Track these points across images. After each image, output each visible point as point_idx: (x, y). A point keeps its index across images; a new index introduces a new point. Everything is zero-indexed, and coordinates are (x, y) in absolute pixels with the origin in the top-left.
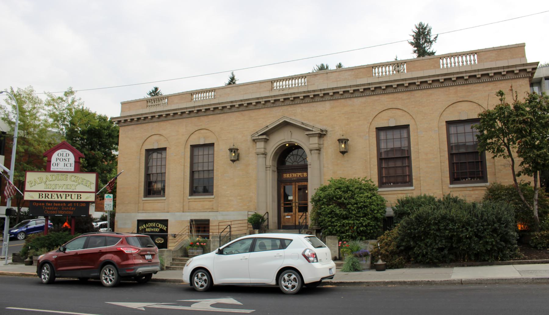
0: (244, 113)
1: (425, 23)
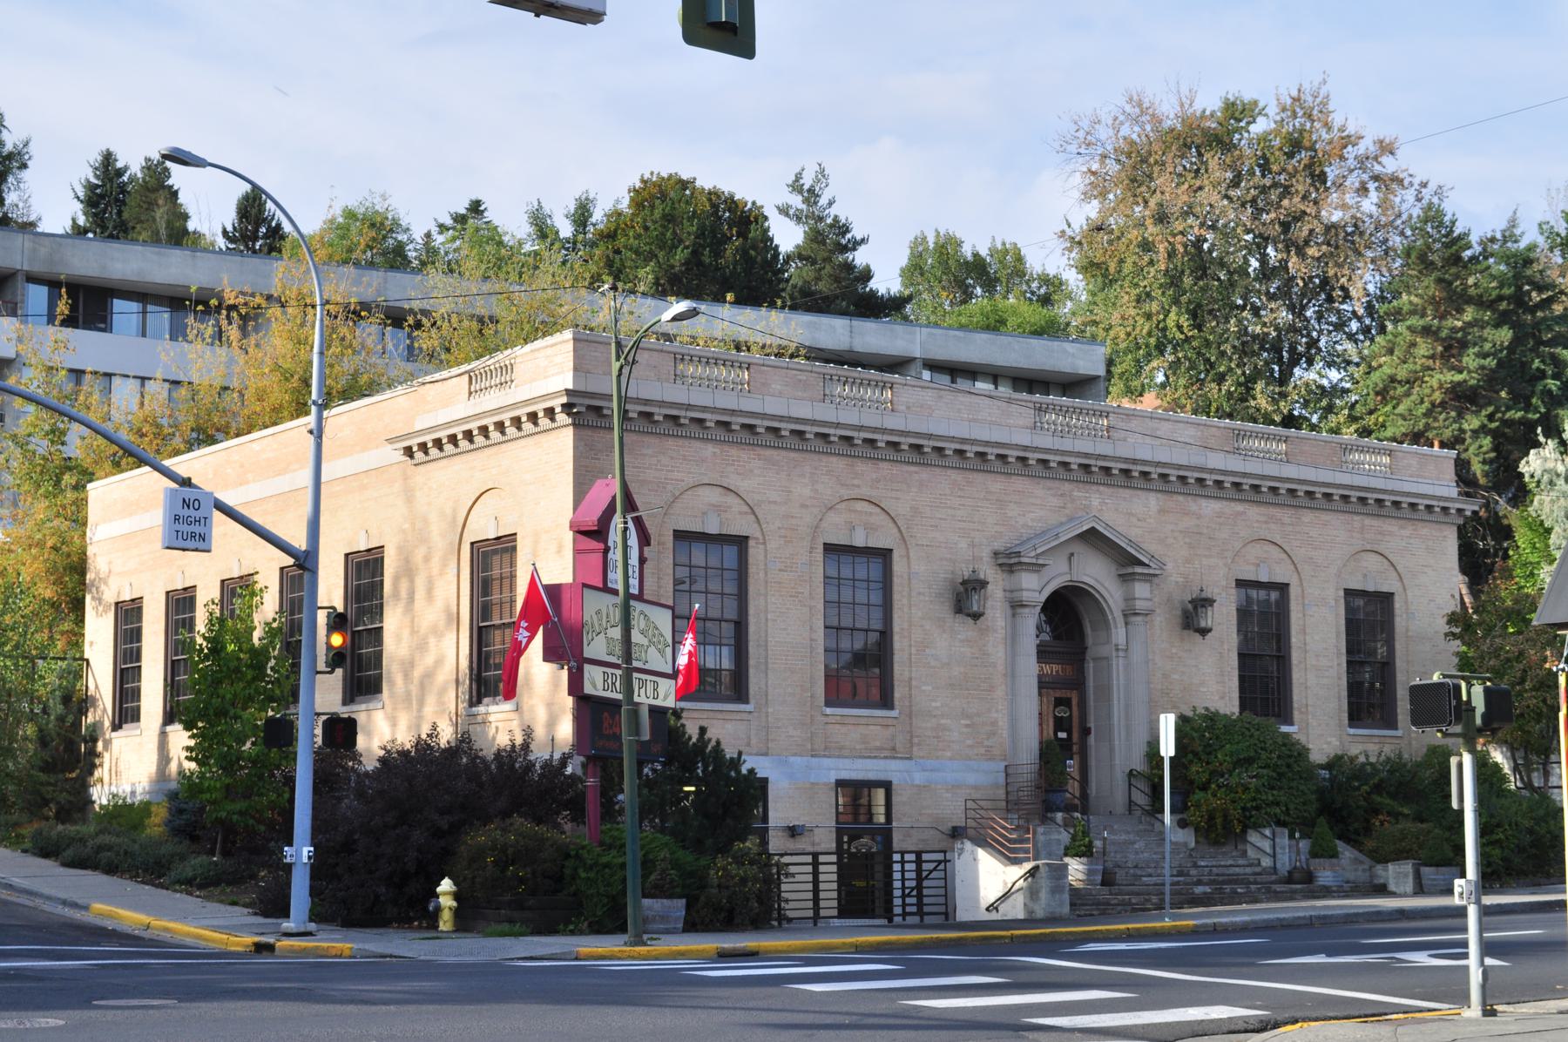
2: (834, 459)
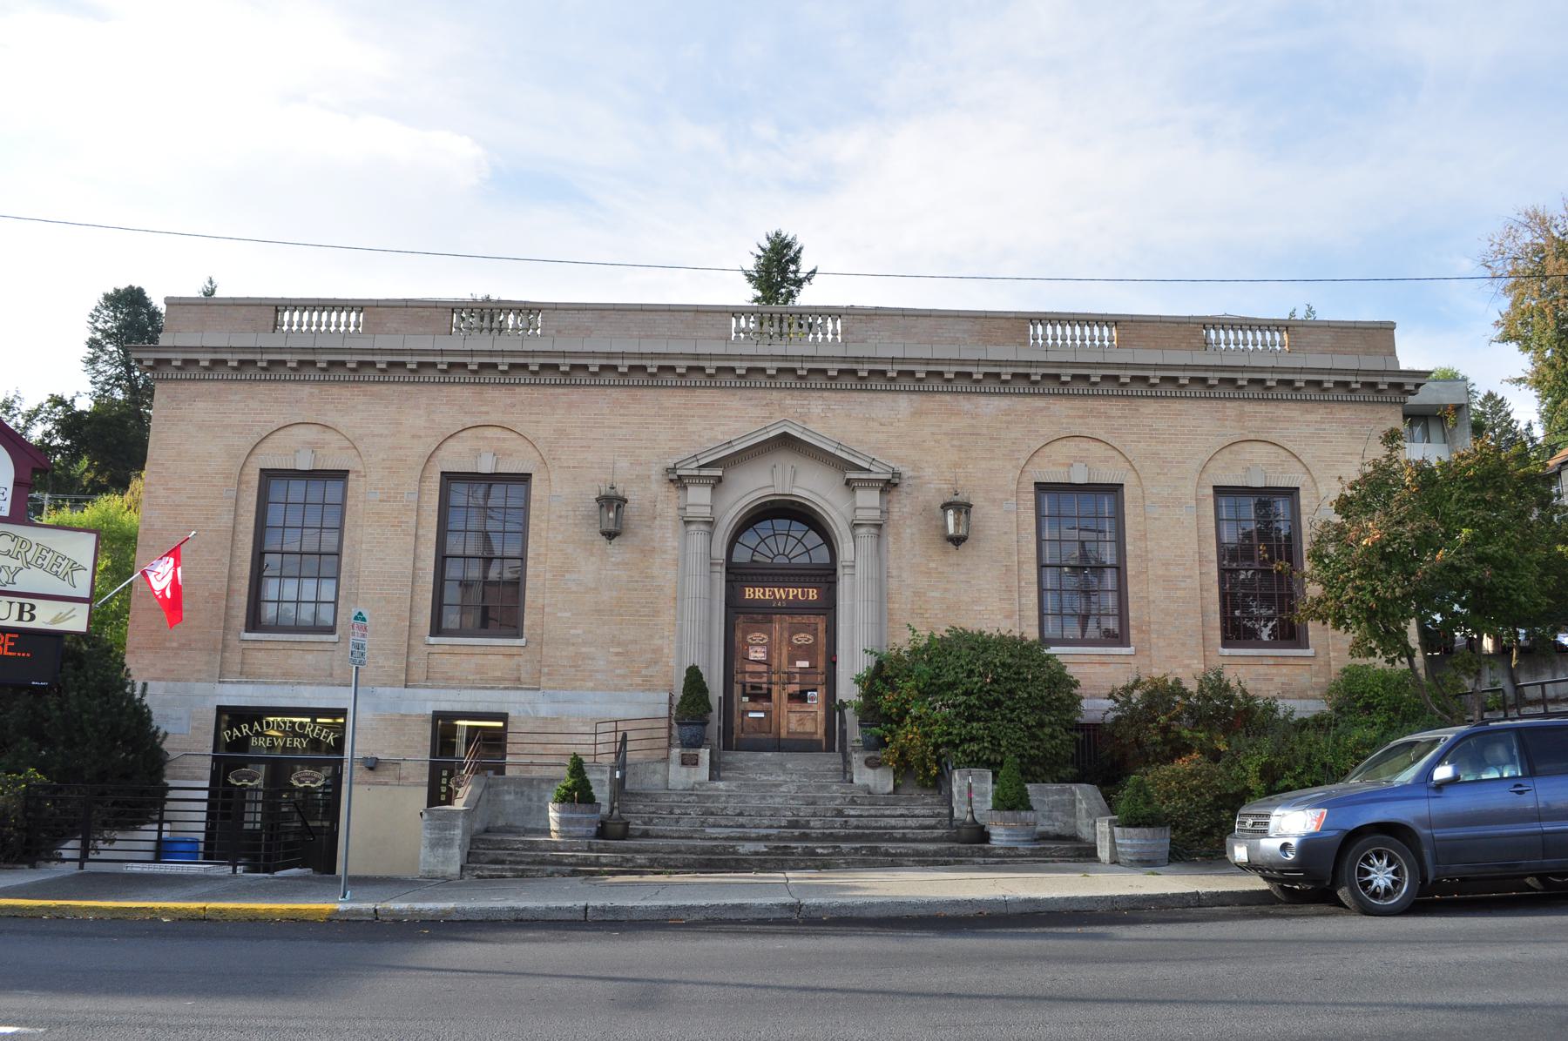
0: (639, 393)
1: (788, 233)
2: (458, 389)
